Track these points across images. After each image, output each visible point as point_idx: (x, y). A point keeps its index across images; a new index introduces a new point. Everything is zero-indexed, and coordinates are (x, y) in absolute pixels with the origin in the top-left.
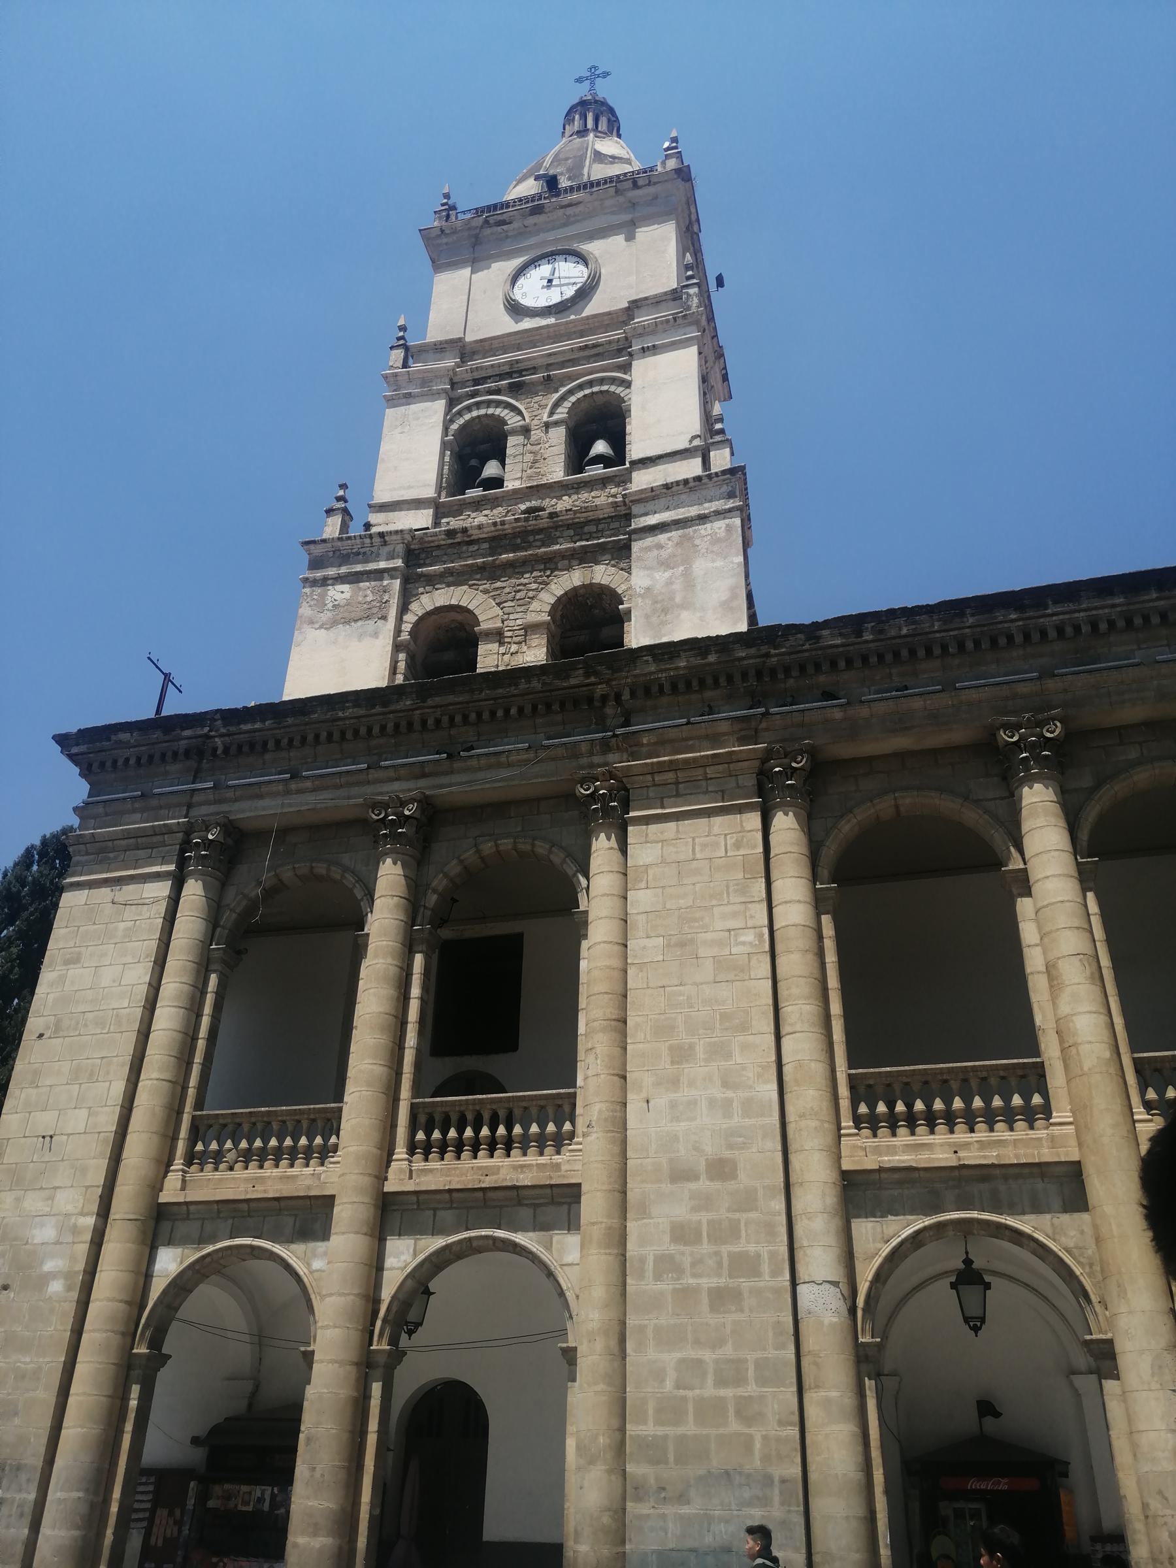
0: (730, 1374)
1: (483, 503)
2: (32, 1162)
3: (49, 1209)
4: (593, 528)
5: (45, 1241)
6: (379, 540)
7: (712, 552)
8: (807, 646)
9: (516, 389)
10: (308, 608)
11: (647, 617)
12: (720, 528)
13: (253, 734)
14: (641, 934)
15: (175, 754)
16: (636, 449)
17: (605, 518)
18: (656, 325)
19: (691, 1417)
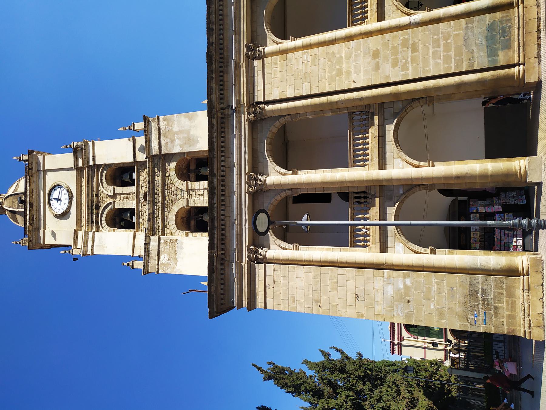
0: (436, 43)
1: (139, 215)
2: (364, 301)
3: (381, 290)
4: (156, 169)
5: (392, 289)
6: (147, 245)
7: (171, 125)
8: (214, 46)
9: (98, 207)
10: (168, 270)
11: (190, 146)
12: (164, 123)
13: (219, 239)
14: (301, 91)
15: (222, 269)
16: (131, 160)
17: (153, 166)
18: (85, 156)
19: (449, 53)
